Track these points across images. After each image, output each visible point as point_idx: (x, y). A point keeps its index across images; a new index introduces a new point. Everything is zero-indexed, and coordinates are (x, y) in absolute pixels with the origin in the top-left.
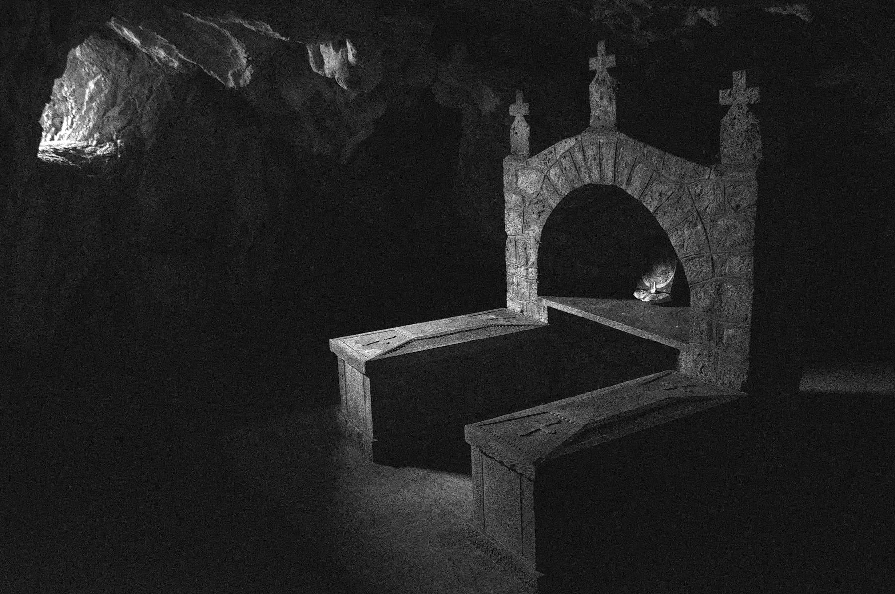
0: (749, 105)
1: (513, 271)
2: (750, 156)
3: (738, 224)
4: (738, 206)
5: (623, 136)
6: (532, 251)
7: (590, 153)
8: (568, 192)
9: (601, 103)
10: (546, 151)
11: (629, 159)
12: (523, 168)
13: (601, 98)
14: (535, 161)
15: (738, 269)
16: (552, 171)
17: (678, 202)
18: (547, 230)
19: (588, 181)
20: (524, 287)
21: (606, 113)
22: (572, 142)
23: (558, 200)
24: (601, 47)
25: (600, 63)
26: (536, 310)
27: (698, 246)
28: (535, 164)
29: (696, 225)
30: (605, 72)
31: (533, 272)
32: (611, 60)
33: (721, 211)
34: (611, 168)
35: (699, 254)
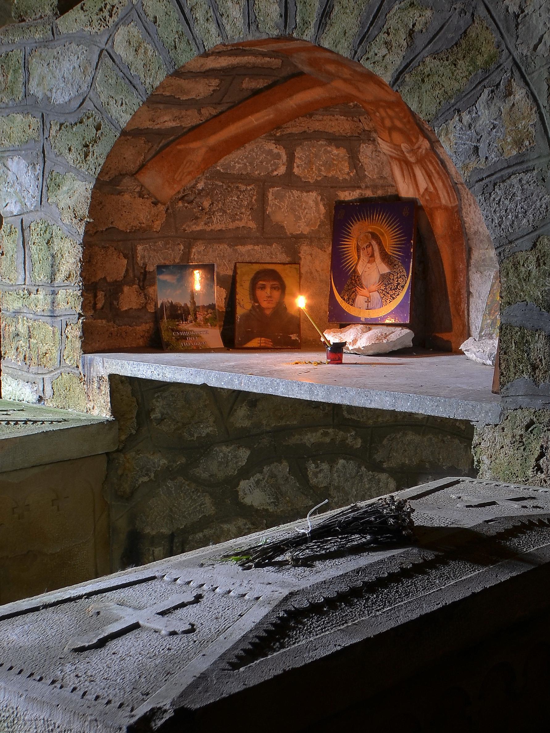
1: (17, 305)
6: (67, 245)
8: (162, 77)
16: (120, 36)
17: (460, 45)
18: (106, 188)
19: (213, 40)
20: (46, 338)
26: (78, 388)
28: (75, 28)
29: (509, 93)
31: (70, 299)
35: (519, 163)
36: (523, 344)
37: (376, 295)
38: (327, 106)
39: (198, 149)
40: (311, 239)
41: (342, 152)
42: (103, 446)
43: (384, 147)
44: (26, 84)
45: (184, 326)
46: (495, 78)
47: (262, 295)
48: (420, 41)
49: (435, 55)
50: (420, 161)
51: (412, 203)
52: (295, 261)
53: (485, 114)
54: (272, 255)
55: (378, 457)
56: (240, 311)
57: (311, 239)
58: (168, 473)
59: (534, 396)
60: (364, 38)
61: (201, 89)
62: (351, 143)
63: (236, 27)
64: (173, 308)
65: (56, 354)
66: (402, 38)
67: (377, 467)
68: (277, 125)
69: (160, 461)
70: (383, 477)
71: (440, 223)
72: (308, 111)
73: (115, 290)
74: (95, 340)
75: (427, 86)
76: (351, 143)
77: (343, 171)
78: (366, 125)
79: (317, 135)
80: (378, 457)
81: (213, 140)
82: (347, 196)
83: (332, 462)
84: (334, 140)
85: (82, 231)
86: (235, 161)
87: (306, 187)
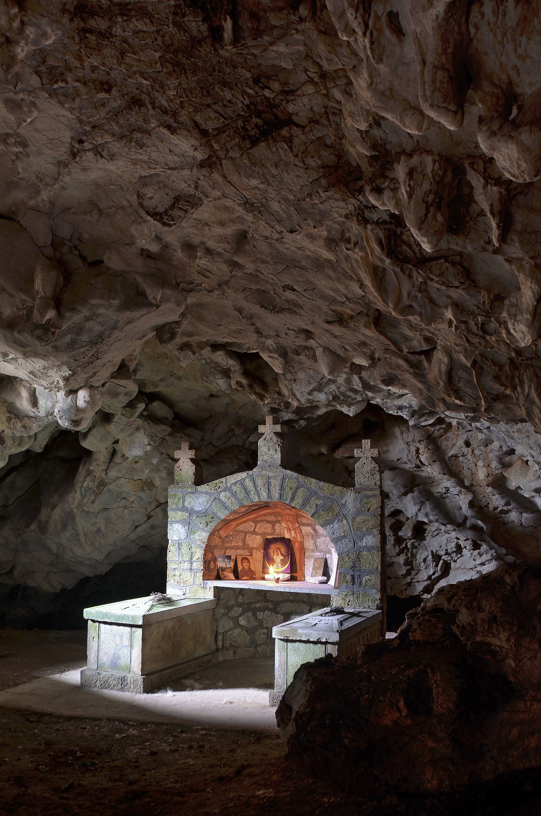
0: (372, 457)
2: (373, 483)
3: (370, 518)
4: (369, 509)
5: (288, 472)
7: (259, 482)
8: (237, 507)
9: (269, 451)
10: (217, 481)
11: (294, 486)
12: (192, 493)
13: (269, 450)
14: (203, 488)
15: (371, 542)
17: (329, 509)
18: (212, 534)
19: (256, 500)
20: (188, 576)
21: (272, 457)
22: (243, 475)
23: (227, 513)
24: (269, 419)
25: (268, 429)
26: (201, 590)
27: (344, 532)
30: (272, 434)
32: (278, 428)
33: (359, 512)
34: (278, 491)
35: (345, 536)
36: (344, 577)
37: (280, 565)
38: (270, 514)
39: (234, 523)
40: (257, 549)
41: (270, 525)
42: (209, 607)
43: (284, 524)
44: (183, 503)
45: (225, 573)
46: (339, 517)
47: (245, 564)
48: (319, 507)
49: (323, 510)
50: (294, 529)
51: (289, 540)
52: (251, 555)
53: (336, 525)
54: (246, 553)
55: (278, 610)
56: (239, 569)
57: (257, 549)
58: (224, 615)
59: (347, 588)
60: (304, 505)
61: (243, 510)
62: (273, 523)
63: (264, 496)
64: (222, 568)
65: (191, 581)
66: (314, 506)
67: (278, 613)
68: (255, 518)
69: (222, 611)
70: (279, 615)
71: (296, 546)
72: (265, 515)
73: (209, 563)
74: (206, 577)
75: (321, 517)
76: (273, 523)
77: (270, 530)
78: (279, 518)
79: (265, 520)
80: (278, 610)
81: (238, 522)
82: (269, 537)
83: (264, 612)
84: (268, 522)
85: (204, 546)
86: (241, 528)
87: (258, 534)
